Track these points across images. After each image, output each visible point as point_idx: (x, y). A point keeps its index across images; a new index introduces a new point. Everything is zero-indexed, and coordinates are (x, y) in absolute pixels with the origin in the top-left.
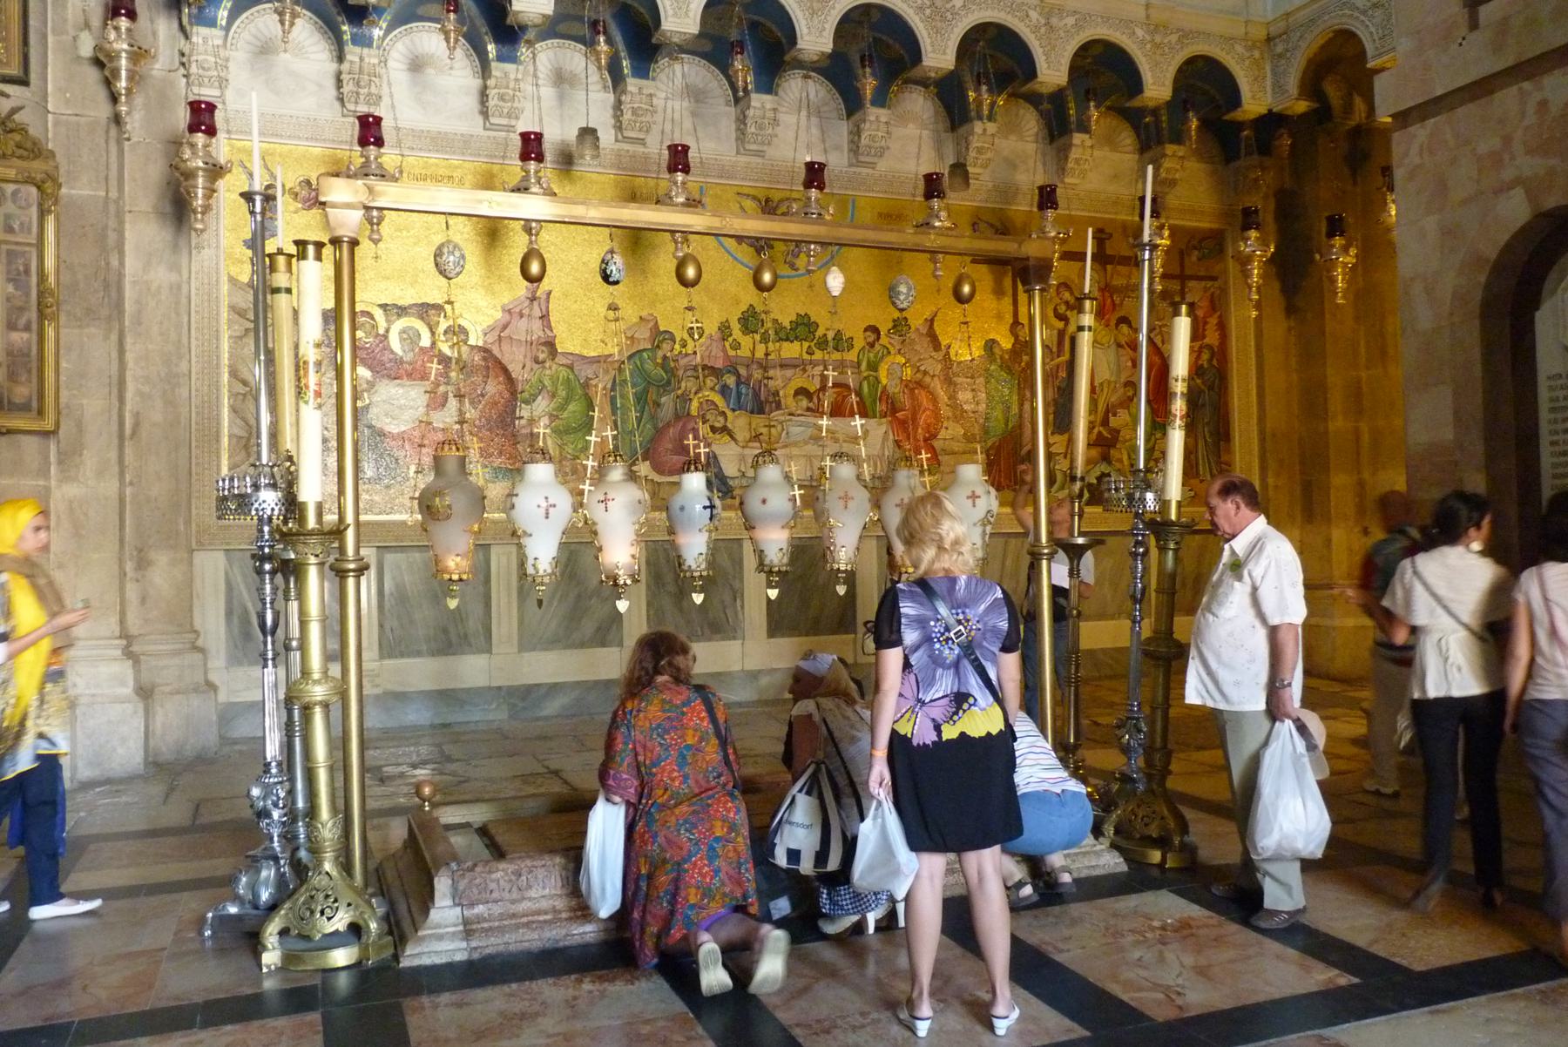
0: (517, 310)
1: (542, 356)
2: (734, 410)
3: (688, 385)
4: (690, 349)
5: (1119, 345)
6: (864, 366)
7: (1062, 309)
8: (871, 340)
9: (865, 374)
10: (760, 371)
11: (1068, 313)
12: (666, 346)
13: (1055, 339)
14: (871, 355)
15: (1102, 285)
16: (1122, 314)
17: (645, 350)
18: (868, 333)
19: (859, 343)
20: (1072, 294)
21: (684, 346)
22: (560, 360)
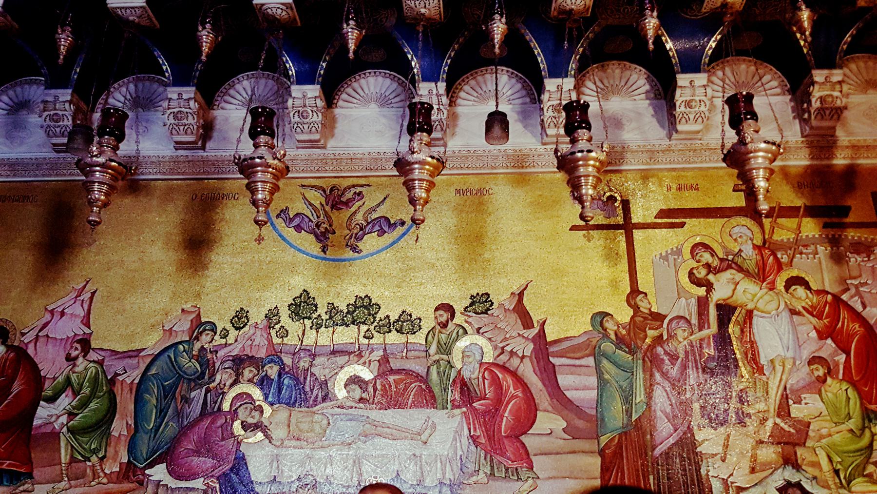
0: (60, 309)
1: (74, 353)
2: (272, 404)
3: (223, 377)
4: (231, 339)
5: (793, 312)
6: (433, 349)
7: (701, 273)
8: (443, 319)
9: (437, 357)
10: (308, 359)
11: (711, 277)
12: (205, 338)
13: (694, 309)
14: (443, 337)
15: (758, 241)
16: (795, 273)
17: (180, 343)
18: (441, 312)
19: (428, 324)
20: (713, 253)
21: (225, 337)
22: (93, 356)
